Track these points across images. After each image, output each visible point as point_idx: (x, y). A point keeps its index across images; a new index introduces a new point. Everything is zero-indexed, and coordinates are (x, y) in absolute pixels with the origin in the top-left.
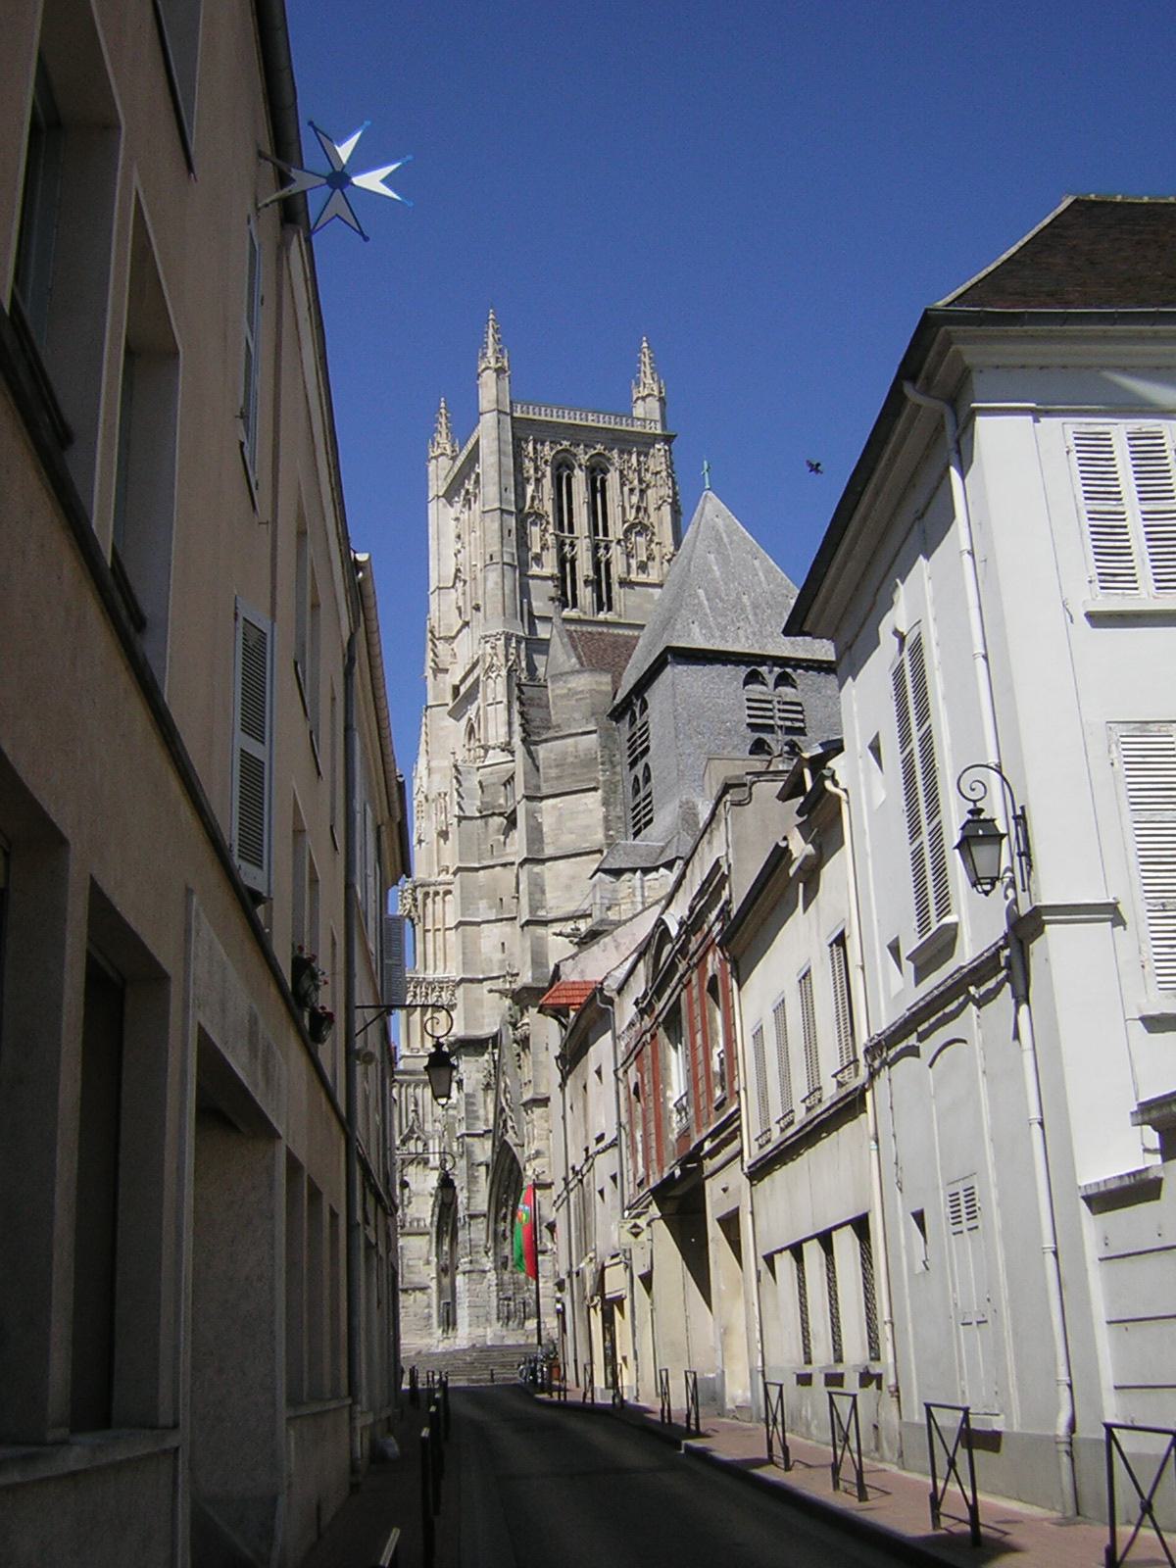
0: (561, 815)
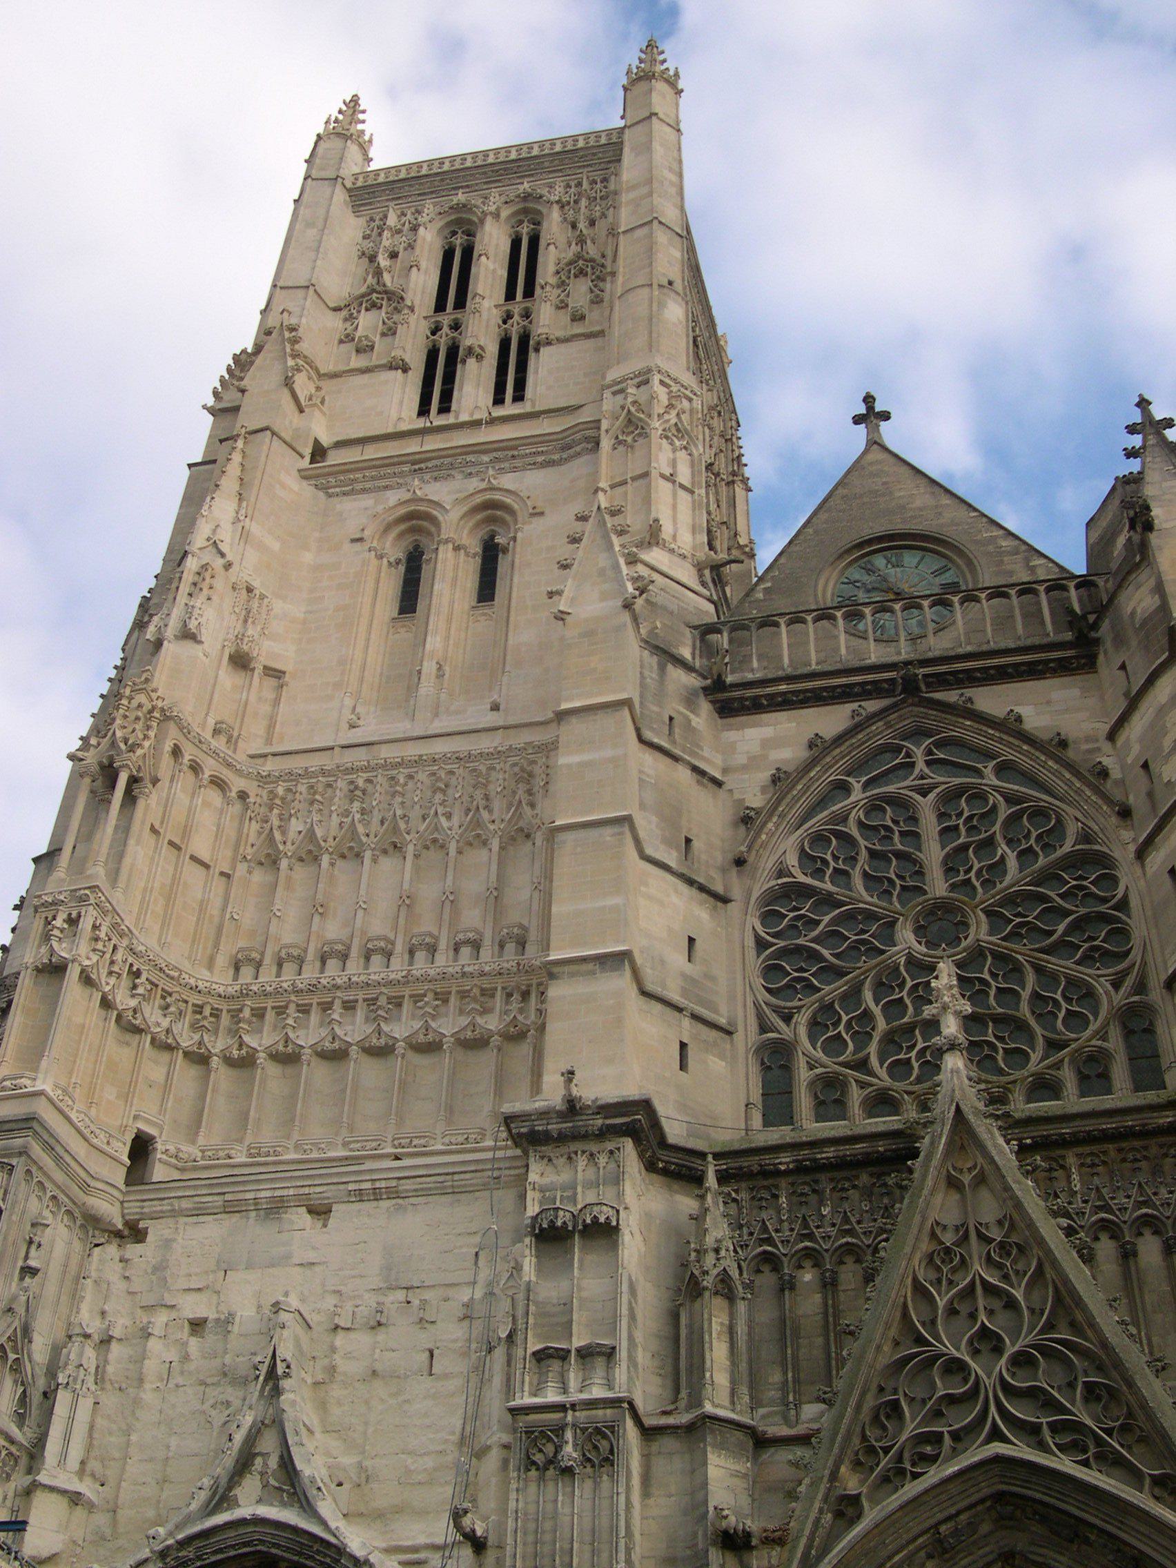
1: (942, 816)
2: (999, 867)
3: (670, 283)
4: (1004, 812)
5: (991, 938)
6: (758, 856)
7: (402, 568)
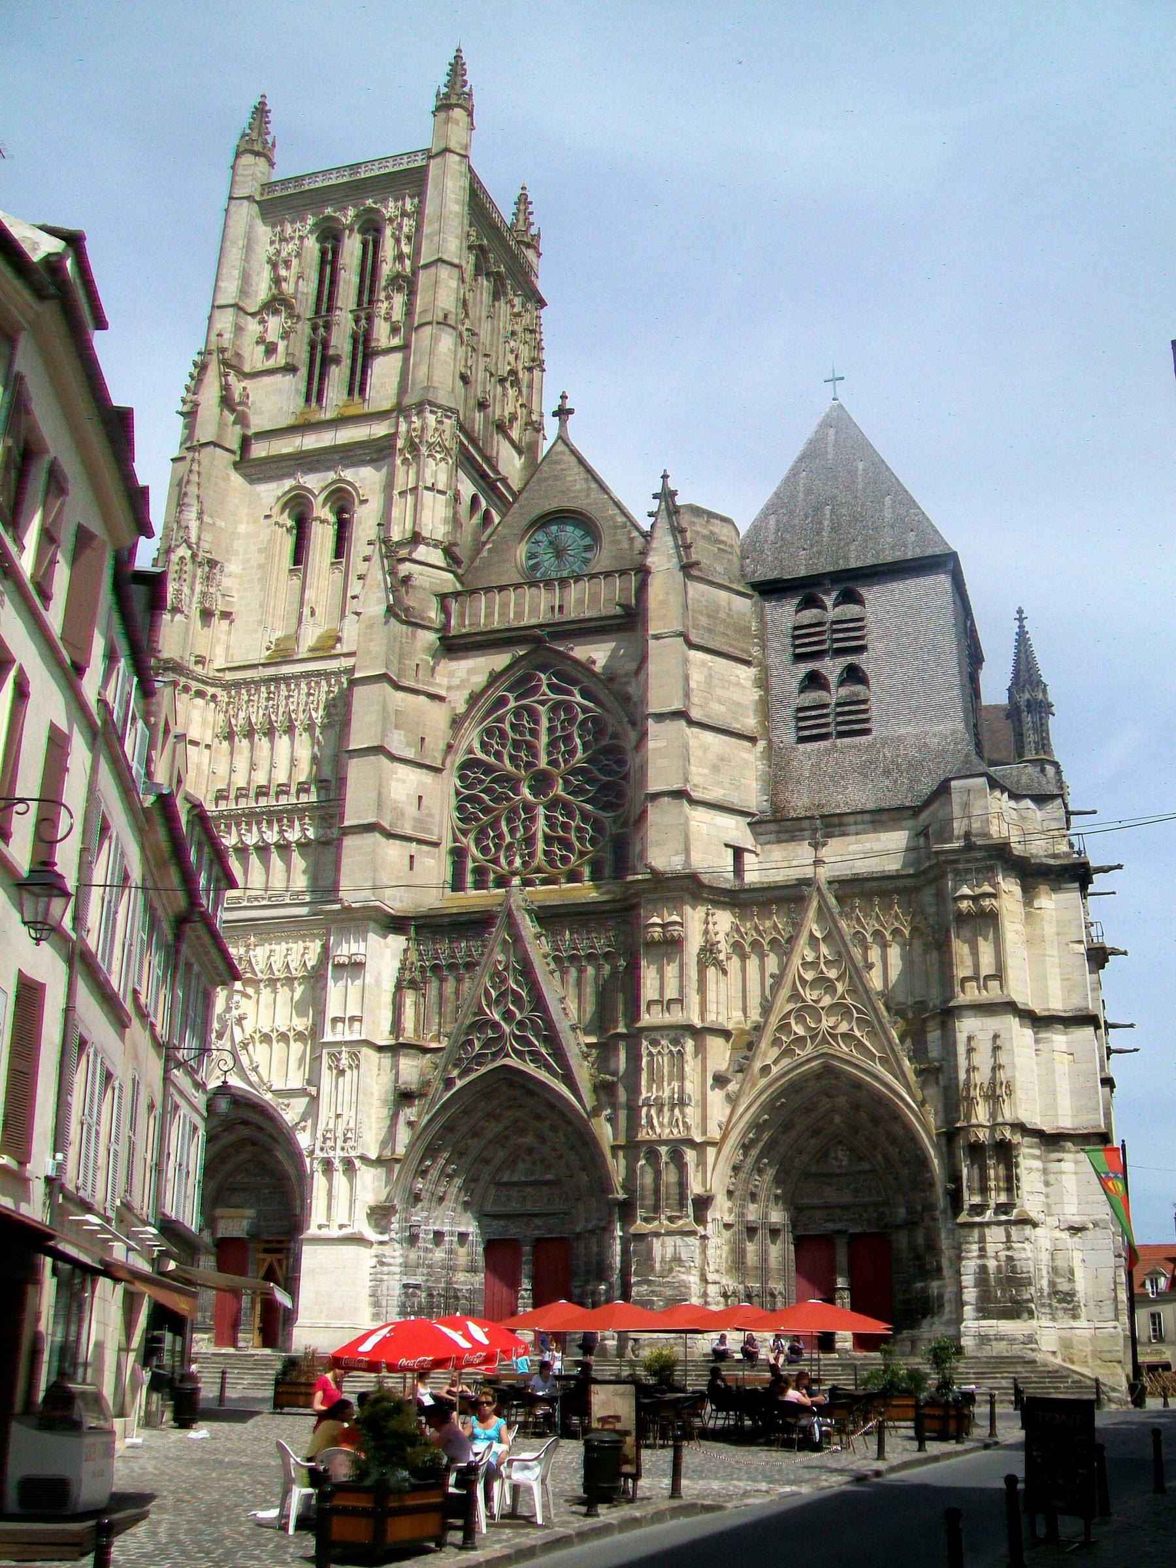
0: (711, 675)
1: (550, 720)
2: (572, 752)
3: (446, 316)
4: (581, 717)
5: (563, 793)
6: (460, 742)
7: (295, 532)
